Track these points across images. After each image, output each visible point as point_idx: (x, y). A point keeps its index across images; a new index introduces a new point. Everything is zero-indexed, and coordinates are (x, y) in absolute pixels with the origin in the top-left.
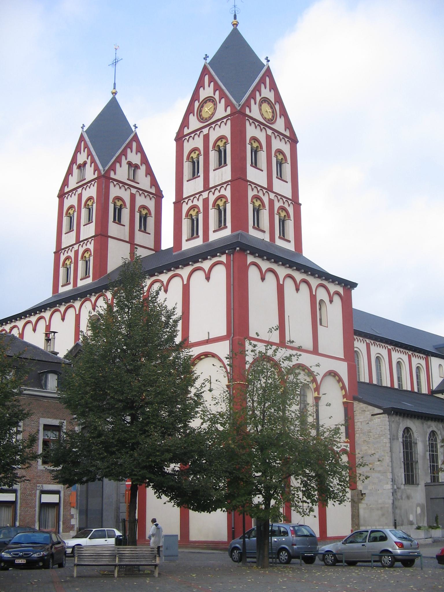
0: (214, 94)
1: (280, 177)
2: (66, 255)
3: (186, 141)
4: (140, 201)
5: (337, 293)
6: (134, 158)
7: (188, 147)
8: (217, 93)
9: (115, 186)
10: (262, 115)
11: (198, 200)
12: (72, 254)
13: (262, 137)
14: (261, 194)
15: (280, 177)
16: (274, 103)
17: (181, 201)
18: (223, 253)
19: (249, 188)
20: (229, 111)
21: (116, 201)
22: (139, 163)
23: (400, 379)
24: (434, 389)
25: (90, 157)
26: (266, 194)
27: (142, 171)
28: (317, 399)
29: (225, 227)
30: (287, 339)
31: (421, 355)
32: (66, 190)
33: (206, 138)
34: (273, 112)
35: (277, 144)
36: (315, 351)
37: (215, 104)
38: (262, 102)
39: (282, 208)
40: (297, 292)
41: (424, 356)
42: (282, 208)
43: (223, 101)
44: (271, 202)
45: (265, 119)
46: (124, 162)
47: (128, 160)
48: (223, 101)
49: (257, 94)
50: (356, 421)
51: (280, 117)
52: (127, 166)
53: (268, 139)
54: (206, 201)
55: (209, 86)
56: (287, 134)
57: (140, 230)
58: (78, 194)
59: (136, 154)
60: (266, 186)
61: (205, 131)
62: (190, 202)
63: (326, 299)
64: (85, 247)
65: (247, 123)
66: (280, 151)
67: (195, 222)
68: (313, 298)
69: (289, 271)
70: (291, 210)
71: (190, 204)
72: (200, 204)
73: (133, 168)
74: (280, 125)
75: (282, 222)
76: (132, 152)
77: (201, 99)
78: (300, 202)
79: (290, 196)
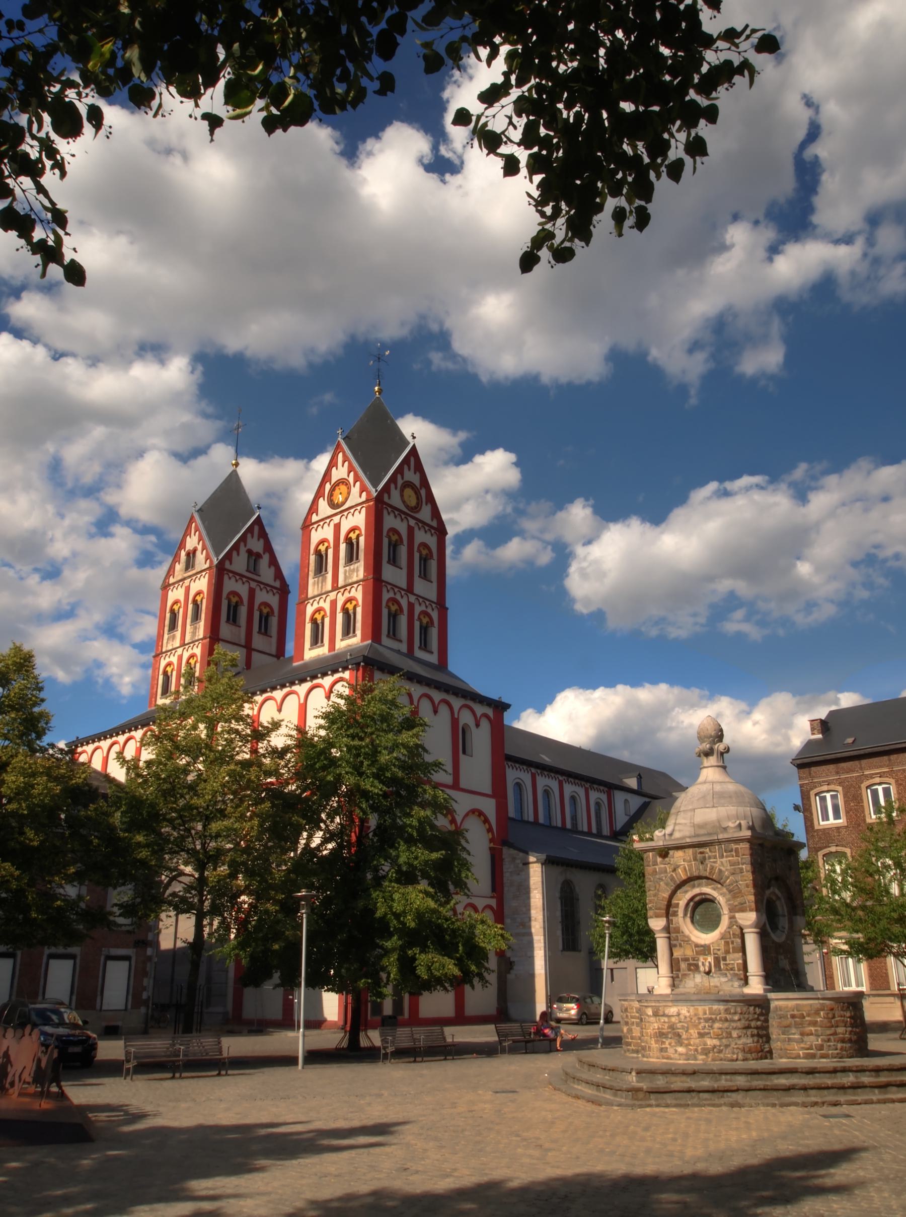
0: (348, 476)
1: (424, 575)
2: (167, 660)
3: (313, 530)
4: (262, 596)
5: (485, 716)
6: (256, 545)
8: (352, 474)
9: (230, 578)
10: (404, 502)
11: (325, 601)
12: (174, 659)
13: (402, 528)
14: (398, 597)
15: (424, 575)
16: (419, 487)
18: (345, 669)
19: (384, 590)
21: (231, 597)
22: (261, 552)
23: (574, 818)
24: (618, 829)
25: (201, 542)
26: (405, 598)
27: (265, 559)
29: (355, 636)
31: (602, 788)
32: (172, 580)
33: (337, 527)
34: (418, 498)
35: (421, 537)
36: (456, 786)
37: (349, 489)
39: (425, 613)
40: (435, 714)
41: (606, 789)
42: (425, 613)
43: (358, 484)
44: (411, 606)
45: (407, 506)
46: (243, 550)
47: (246, 549)
48: (358, 484)
49: (399, 476)
50: (505, 870)
51: (426, 504)
53: (411, 530)
54: (334, 603)
55: (343, 466)
56: (434, 524)
57: (260, 632)
58: (186, 587)
59: (259, 540)
60: (404, 586)
61: (336, 519)
62: (315, 603)
63: (471, 722)
64: (190, 652)
65: (385, 512)
66: (424, 545)
67: (320, 627)
68: (455, 722)
69: (425, 690)
70: (435, 615)
71: (316, 606)
72: (327, 606)
73: (254, 558)
74: (425, 514)
75: (424, 630)
77: (334, 480)
78: (447, 605)
79: (434, 599)
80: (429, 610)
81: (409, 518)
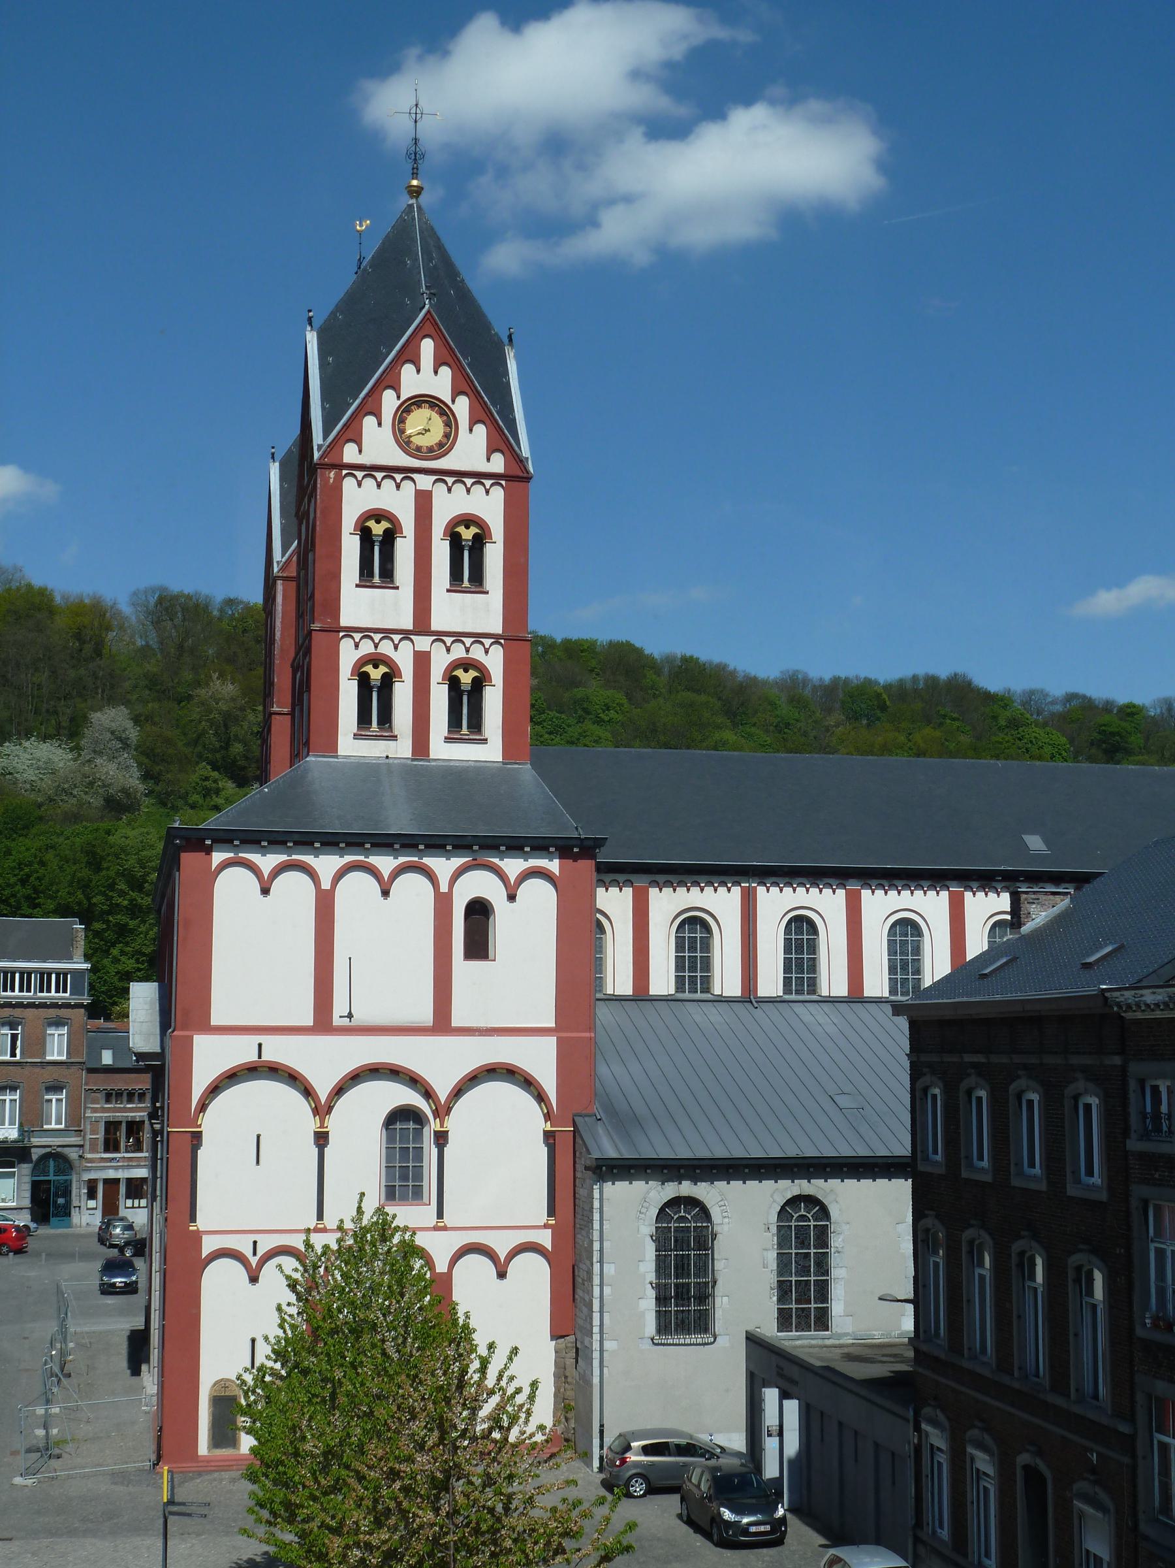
14: (386, 648)
19: (346, 646)
28: (441, 1138)
30: (339, 1008)
36: (442, 1023)
38: (408, 411)
44: (422, 661)
45: (417, 452)
53: (423, 502)
60: (408, 624)
68: (443, 903)
80: (477, 653)
81: (415, 476)
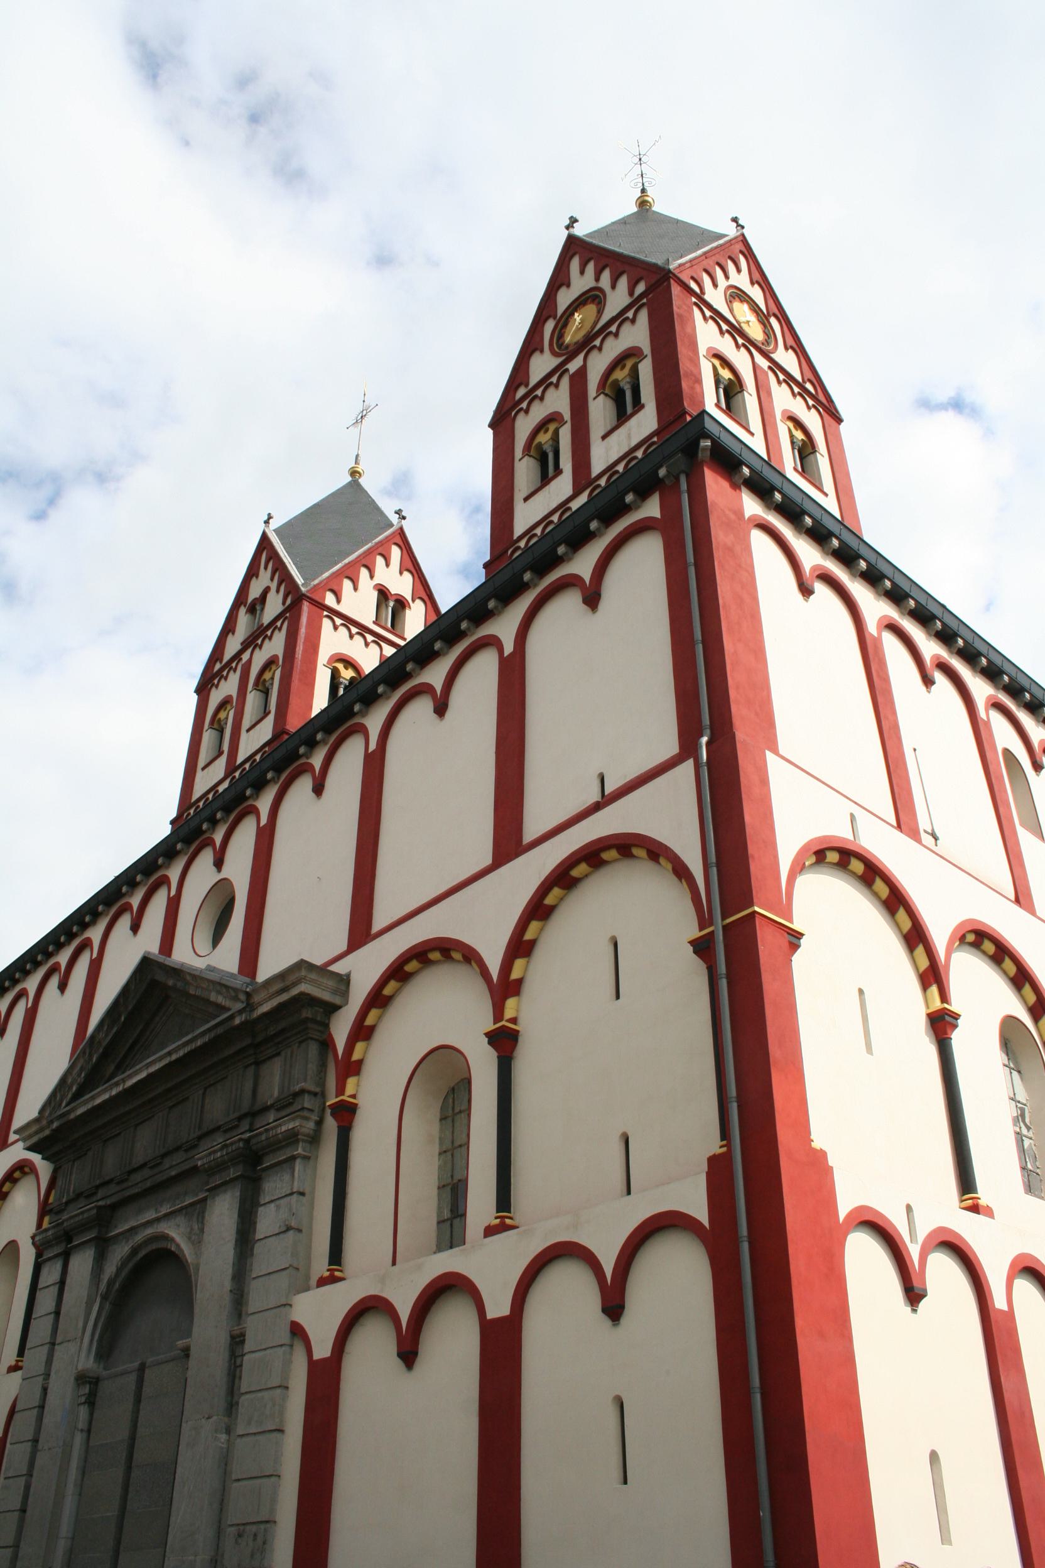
7: (524, 426)
9: (336, 628)
17: (506, 552)
20: (641, 288)
22: (409, 598)
47: (376, 580)
52: (376, 593)
55: (582, 272)
61: (574, 366)
76: (388, 565)
